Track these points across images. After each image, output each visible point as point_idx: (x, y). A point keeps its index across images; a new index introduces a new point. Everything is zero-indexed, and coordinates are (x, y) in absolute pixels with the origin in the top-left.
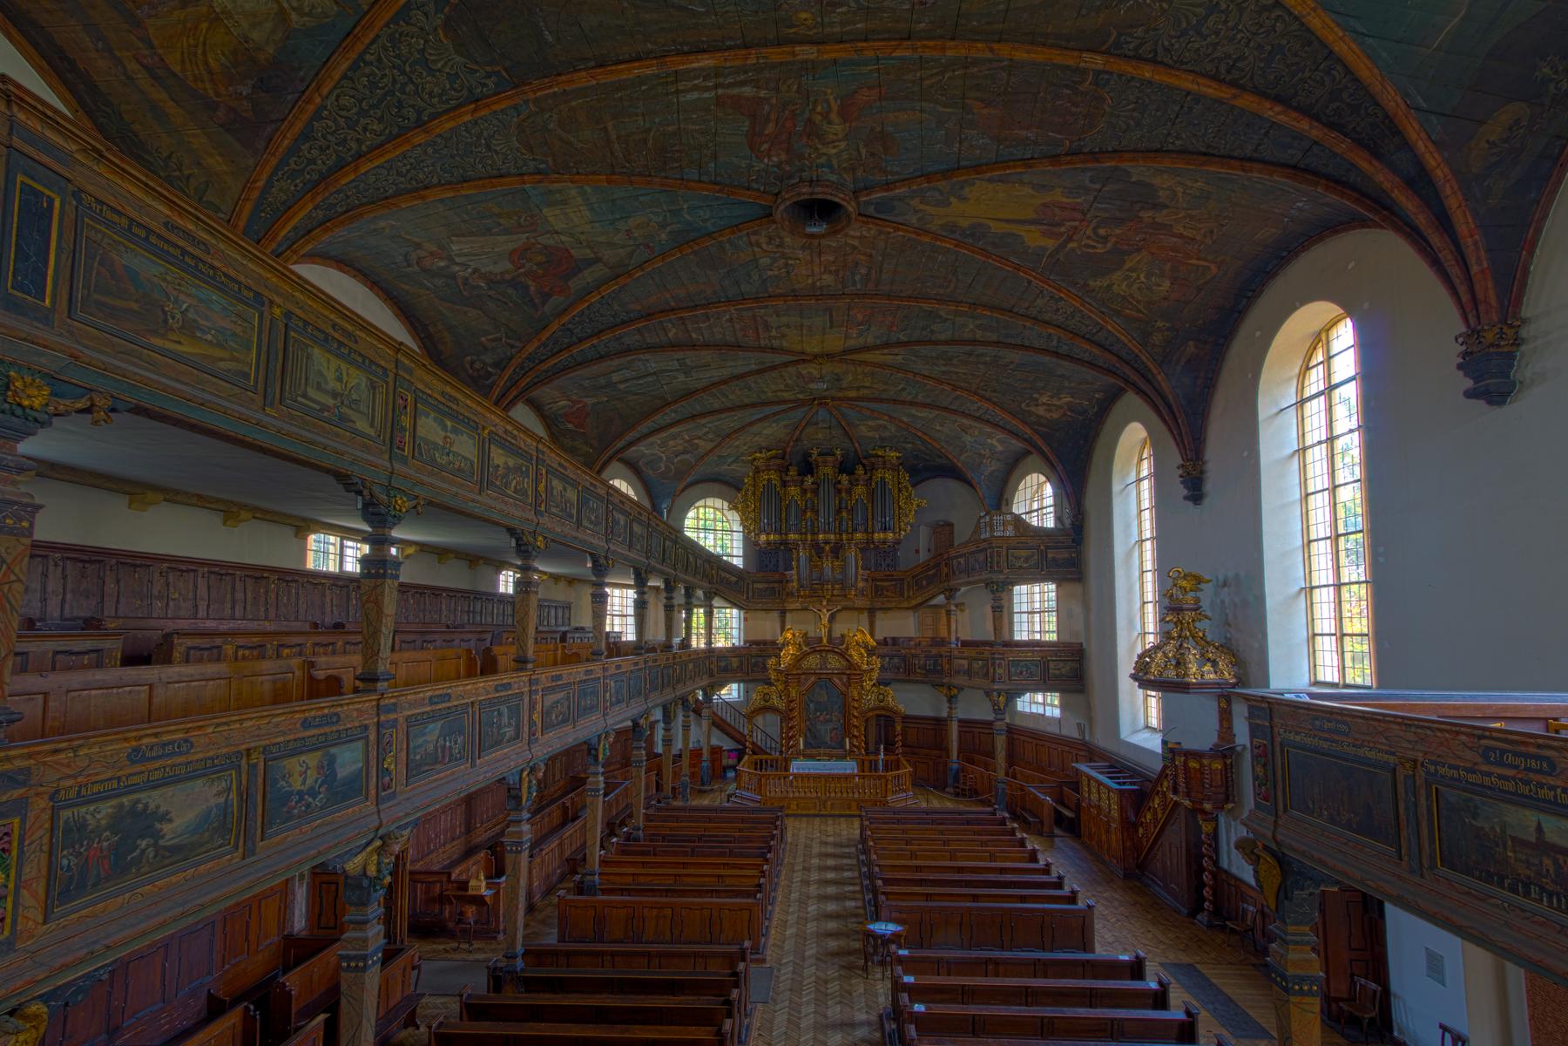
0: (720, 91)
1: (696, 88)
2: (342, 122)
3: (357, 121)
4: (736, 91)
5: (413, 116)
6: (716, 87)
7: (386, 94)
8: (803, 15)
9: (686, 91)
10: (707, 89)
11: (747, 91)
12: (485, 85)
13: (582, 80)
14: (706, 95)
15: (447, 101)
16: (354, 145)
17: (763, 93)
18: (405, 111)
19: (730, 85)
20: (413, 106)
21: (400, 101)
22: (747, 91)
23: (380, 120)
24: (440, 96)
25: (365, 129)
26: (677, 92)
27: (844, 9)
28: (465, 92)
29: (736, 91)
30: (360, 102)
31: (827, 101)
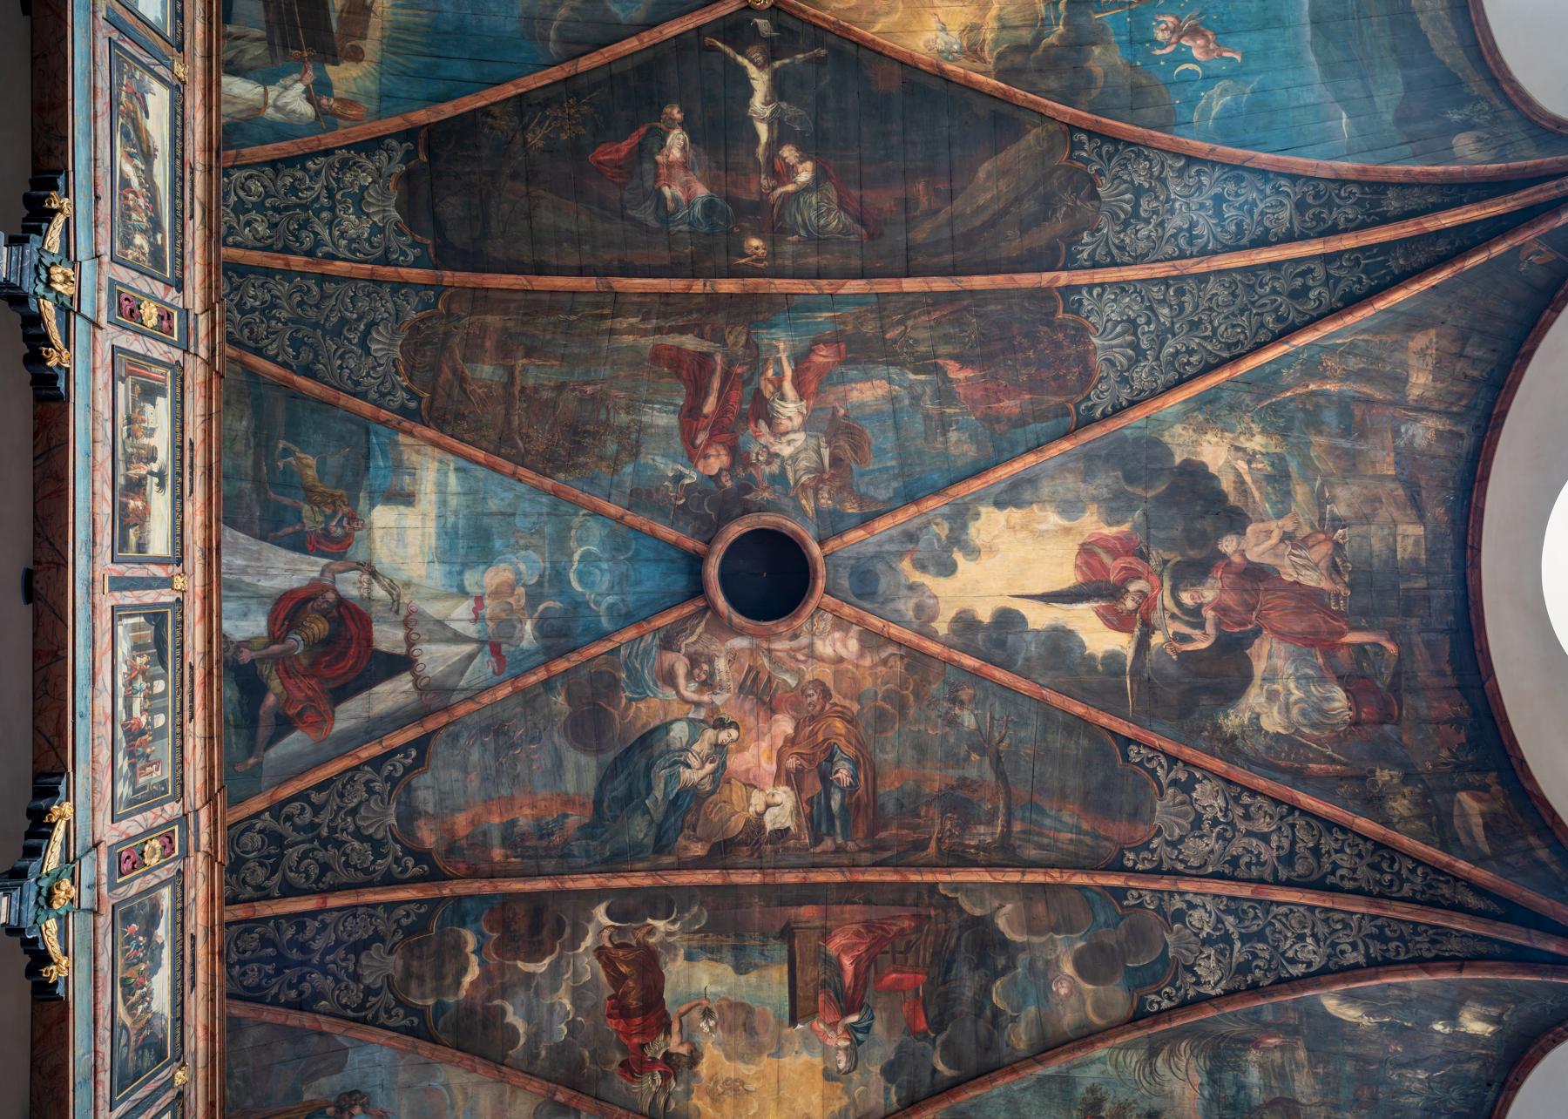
1: (631, 330)
2: (233, 199)
3: (249, 211)
5: (308, 241)
7: (297, 206)
9: (622, 333)
10: (645, 333)
11: (690, 342)
12: (405, 254)
15: (353, 252)
18: (304, 234)
19: (672, 330)
20: (316, 234)
21: (307, 221)
23: (273, 226)
24: (351, 240)
25: (248, 223)
26: (612, 332)
27: (796, 238)
28: (379, 252)
30: (268, 195)
31: (778, 361)
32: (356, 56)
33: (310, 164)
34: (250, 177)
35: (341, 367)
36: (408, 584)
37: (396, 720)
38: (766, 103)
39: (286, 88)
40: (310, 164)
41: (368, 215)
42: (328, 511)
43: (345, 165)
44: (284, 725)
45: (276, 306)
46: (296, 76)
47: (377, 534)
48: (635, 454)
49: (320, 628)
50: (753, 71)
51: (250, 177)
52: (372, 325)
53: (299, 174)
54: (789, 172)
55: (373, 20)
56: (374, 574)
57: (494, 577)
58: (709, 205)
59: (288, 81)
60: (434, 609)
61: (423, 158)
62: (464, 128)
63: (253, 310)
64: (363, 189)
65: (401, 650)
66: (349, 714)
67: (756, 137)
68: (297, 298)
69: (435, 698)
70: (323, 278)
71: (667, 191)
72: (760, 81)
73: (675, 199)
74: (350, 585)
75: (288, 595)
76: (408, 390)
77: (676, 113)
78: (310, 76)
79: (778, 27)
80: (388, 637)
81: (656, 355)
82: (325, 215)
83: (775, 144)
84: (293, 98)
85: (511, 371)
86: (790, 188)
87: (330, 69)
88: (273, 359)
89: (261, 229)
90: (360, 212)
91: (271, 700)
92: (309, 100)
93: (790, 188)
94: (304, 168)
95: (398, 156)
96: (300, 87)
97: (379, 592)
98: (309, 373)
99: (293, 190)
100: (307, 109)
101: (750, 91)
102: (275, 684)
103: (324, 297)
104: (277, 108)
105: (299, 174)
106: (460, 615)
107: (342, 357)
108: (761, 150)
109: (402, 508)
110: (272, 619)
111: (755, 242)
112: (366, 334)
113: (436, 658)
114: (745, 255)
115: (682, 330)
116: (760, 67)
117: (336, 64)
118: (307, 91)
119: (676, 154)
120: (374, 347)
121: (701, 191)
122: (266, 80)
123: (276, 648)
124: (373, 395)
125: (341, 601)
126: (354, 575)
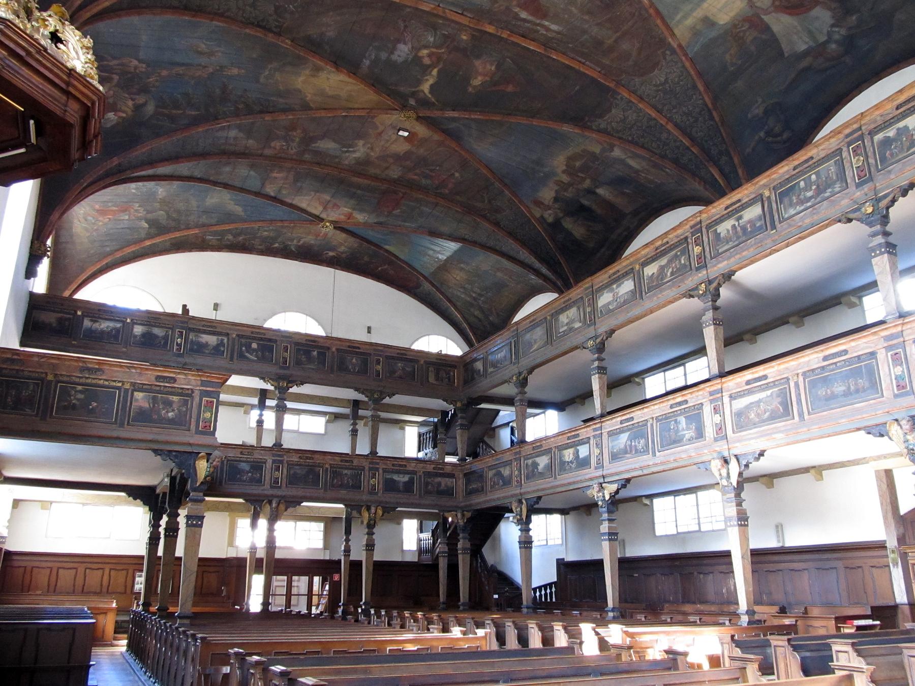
1: (547, 29)
4: (530, 18)
6: (538, 25)
8: (465, 38)
11: (524, 15)
14: (547, 23)
17: (517, 10)
22: (524, 15)
26: (558, 33)
29: (530, 18)
38: (427, 80)
43: (618, 132)
47: (732, 14)
50: (427, 91)
52: (655, 85)
54: (429, 56)
58: (478, 57)
62: (563, 118)
67: (439, 72)
70: (659, 111)
71: (493, 68)
72: (426, 87)
73: (492, 65)
76: (665, 59)
77: (470, 89)
79: (407, 100)
81: (545, 16)
83: (432, 66)
85: (616, 41)
86: (434, 50)
88: (703, 99)
90: (625, 118)
93: (434, 50)
95: (596, 123)
98: (695, 87)
99: (642, 137)
101: (432, 86)
103: (664, 105)
107: (678, 83)
108: (440, 66)
109: (711, 18)
111: (465, 38)
112: (661, 84)
114: (473, 35)
115: (524, 20)
116: (423, 91)
119: (480, 78)
121: (477, 63)
124: (680, 65)
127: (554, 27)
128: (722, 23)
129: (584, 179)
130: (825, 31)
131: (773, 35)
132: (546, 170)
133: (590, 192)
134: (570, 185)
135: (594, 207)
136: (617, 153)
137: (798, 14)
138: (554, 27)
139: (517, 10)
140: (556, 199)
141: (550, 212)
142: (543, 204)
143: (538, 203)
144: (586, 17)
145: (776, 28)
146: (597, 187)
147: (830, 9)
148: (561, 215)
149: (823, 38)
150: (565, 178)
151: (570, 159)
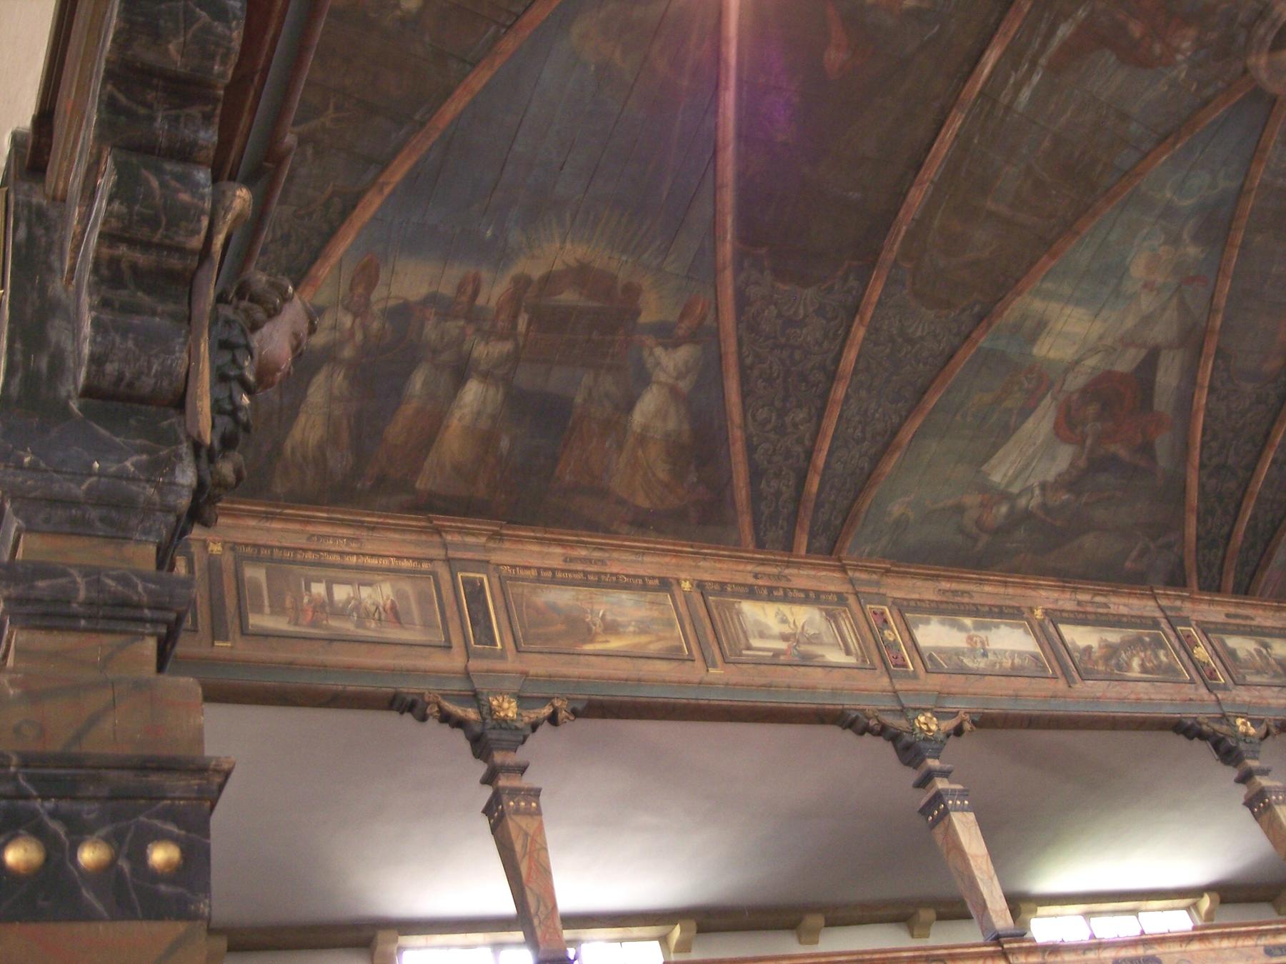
0: (1043, 61)
4: (1055, 43)
6: (1034, 64)
11: (1064, 31)
13: (917, 197)
14: (1036, 79)
16: (799, 449)
17: (1081, 14)
19: (1044, 45)
22: (1064, 31)
25: (795, 425)
29: (1055, 43)
32: (632, 292)
33: (749, 361)
34: (754, 416)
35: (925, 364)
36: (1101, 338)
37: (1190, 374)
39: (658, 364)
40: (749, 361)
41: (806, 316)
42: (1016, 388)
44: (1147, 449)
45: (866, 411)
46: (646, 353)
47: (1052, 355)
48: (1124, 117)
49: (1092, 409)
51: (754, 416)
53: (756, 372)
55: (597, 265)
56: (1077, 363)
57: (1138, 269)
59: (650, 362)
60: (1130, 322)
61: (763, 251)
63: (863, 431)
64: (779, 315)
65: (1143, 353)
66: (1164, 400)
68: (863, 393)
69: (1192, 340)
74: (1076, 382)
75: (1056, 427)
76: (964, 310)
78: (650, 341)
80: (1126, 363)
82: (798, 355)
84: (671, 362)
87: (644, 319)
88: (904, 420)
89: (801, 415)
91: (1123, 453)
92: (676, 345)
94: (751, 368)
96: (659, 351)
97: (1091, 362)
100: (684, 354)
102: (1113, 448)
104: (680, 376)
105: (756, 372)
106: (1147, 303)
110: (1067, 440)
113: (1163, 331)
117: (637, 313)
118: (666, 347)
120: (919, 333)
122: (644, 379)
123: (1089, 442)
125: (1084, 391)
126: (1070, 377)
127: (1025, 94)
128: (1035, 351)
129: (510, 334)
130: (1031, 481)
131: (1016, 429)
132: (515, 236)
133: (461, 372)
134: (472, 315)
135: (408, 409)
136: (671, 362)
137: (1057, 434)
138: (1025, 94)
139: (1081, 14)
140: (402, 313)
141: (347, 321)
142: (371, 285)
143: (367, 275)
144: (1046, 144)
145: (1030, 424)
146: (485, 376)
147: (1072, 465)
148: (347, 353)
149: (1015, 489)
150: (494, 292)
151: (582, 275)
